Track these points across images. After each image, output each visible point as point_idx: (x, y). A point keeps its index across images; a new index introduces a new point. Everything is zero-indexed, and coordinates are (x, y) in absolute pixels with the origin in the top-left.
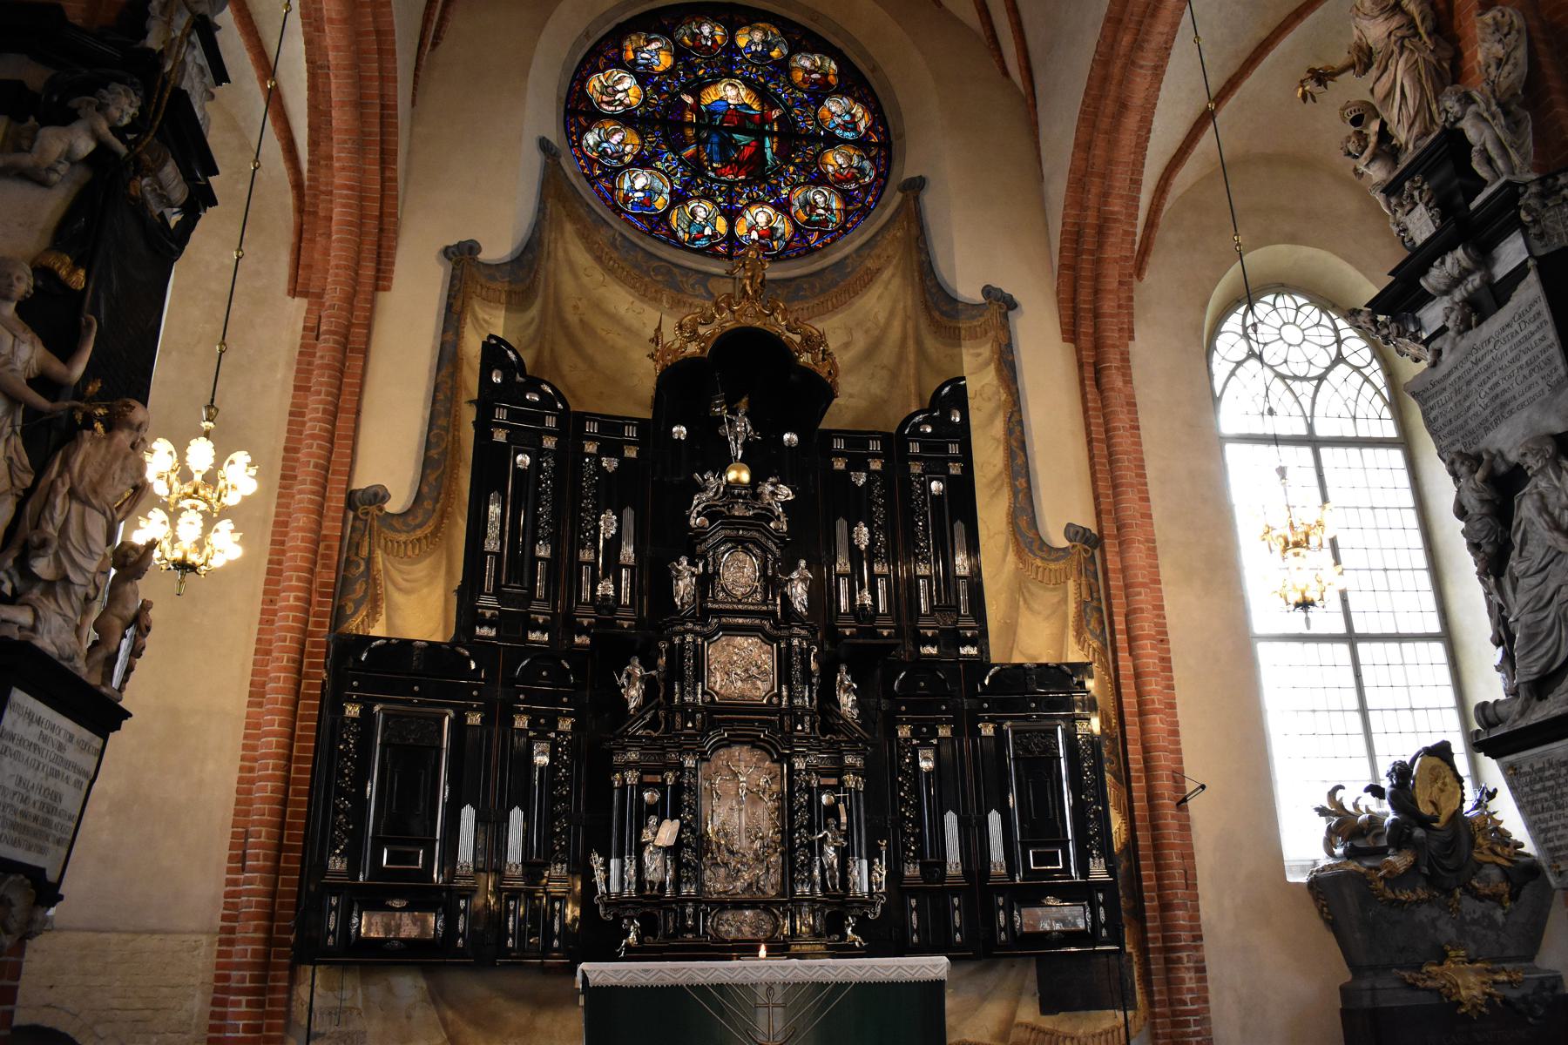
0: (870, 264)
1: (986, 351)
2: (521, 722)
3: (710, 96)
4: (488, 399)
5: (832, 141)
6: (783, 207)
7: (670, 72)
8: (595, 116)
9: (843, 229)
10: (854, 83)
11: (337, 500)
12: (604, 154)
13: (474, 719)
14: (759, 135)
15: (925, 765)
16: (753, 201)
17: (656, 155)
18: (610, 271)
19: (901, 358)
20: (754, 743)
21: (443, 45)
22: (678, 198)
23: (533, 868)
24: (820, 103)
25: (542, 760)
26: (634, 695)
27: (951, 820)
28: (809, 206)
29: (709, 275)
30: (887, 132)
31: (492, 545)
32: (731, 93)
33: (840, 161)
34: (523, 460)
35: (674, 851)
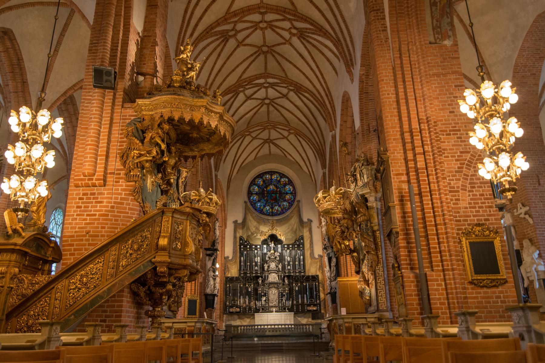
1: (307, 229)
2: (247, 286)
3: (268, 189)
4: (241, 245)
5: (287, 193)
6: (280, 206)
7: (262, 185)
8: (252, 194)
9: (289, 209)
11: (223, 259)
13: (242, 286)
14: (276, 194)
16: (275, 206)
21: (230, 188)
22: (265, 206)
23: (249, 303)
26: (260, 282)
27: (300, 296)
28: (284, 205)
29: (268, 220)
31: (242, 264)
32: (272, 187)
34: (245, 252)
35: (265, 300)
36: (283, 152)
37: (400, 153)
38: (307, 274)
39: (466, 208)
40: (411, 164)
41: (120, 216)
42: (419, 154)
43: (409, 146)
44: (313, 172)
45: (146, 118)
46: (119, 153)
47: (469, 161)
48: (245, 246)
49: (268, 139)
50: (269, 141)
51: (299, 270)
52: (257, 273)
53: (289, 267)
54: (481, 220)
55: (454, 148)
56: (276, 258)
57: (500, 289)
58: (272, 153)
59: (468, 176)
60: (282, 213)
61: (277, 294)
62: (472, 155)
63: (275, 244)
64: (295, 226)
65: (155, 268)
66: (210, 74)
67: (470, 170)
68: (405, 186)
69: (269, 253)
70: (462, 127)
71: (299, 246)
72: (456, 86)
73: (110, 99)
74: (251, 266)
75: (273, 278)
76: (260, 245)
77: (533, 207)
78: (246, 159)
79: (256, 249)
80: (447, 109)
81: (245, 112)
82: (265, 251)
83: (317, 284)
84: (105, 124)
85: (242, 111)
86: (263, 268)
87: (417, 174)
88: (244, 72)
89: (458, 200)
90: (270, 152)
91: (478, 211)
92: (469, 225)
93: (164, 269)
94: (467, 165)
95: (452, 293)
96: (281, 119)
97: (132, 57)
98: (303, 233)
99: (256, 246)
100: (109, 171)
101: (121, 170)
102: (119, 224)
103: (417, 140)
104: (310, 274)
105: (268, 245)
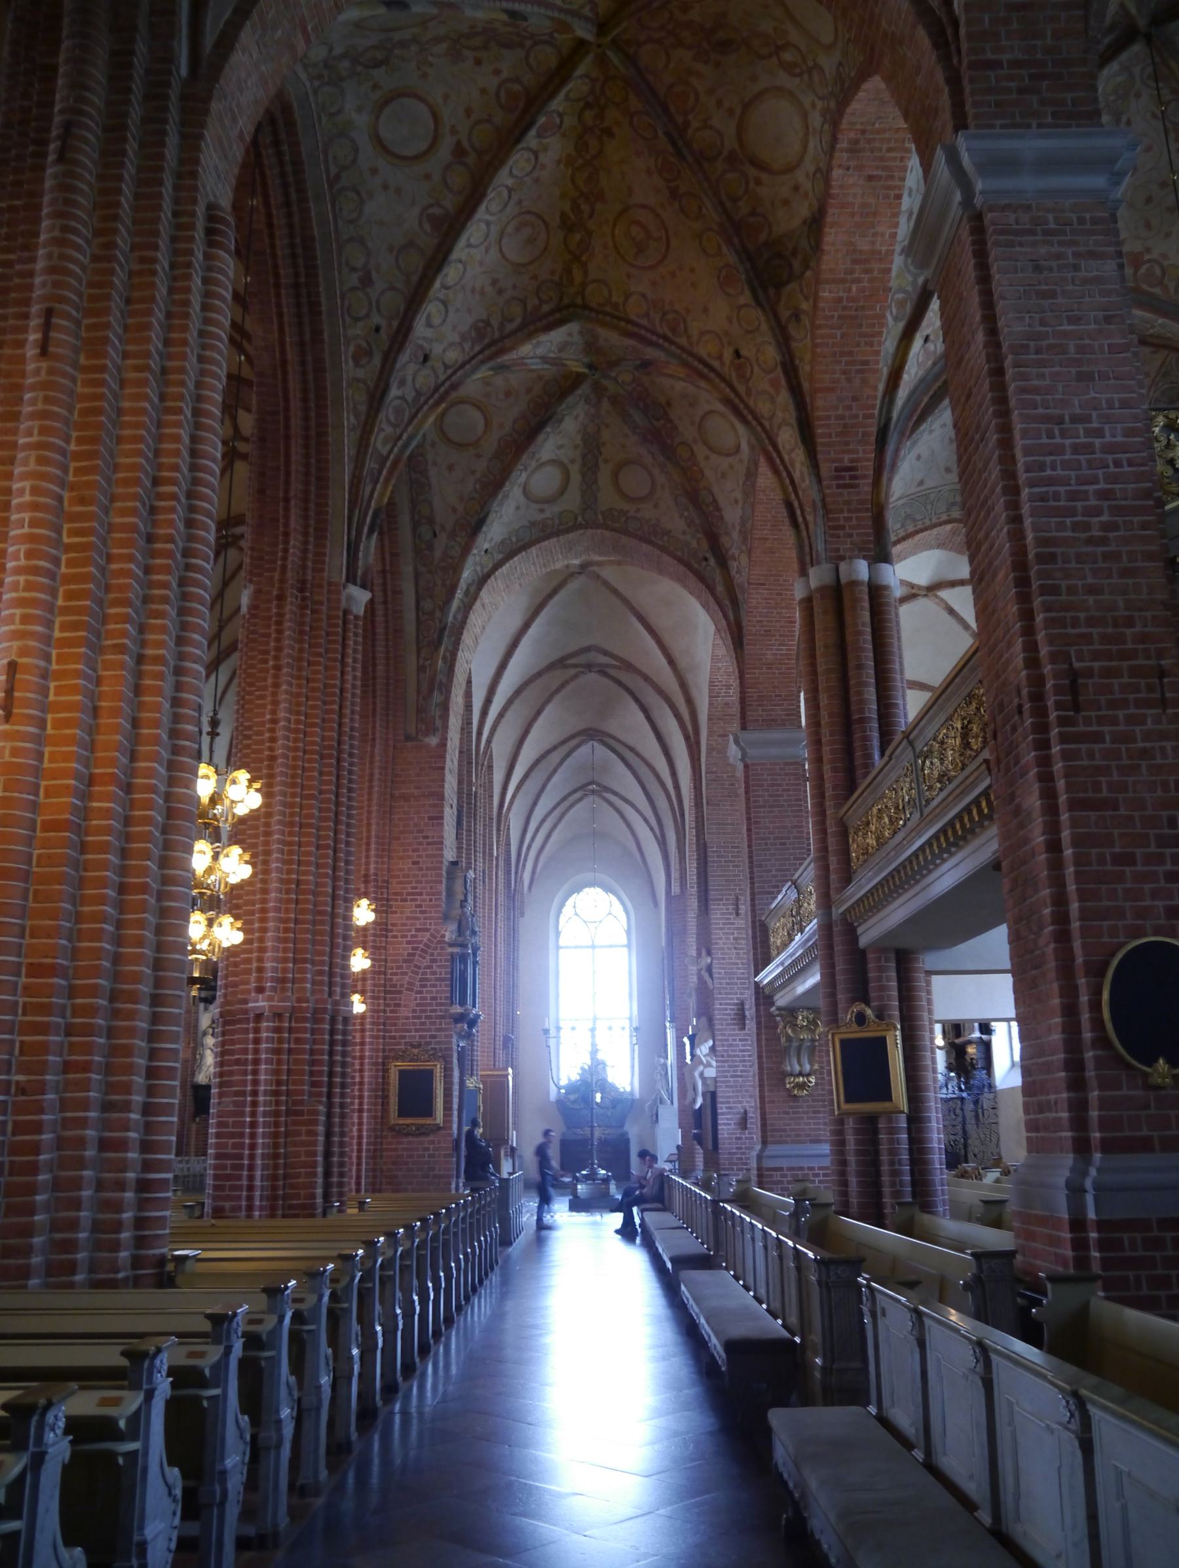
39: (407, 1018)
47: (426, 945)
54: (425, 1037)
55: (409, 922)
57: (431, 1138)
59: (419, 968)
62: (432, 935)
67: (424, 958)
70: (425, 888)
72: (430, 818)
77: (718, 959)
80: (409, 857)
89: (398, 1005)
91: (423, 1024)
92: (406, 1043)
94: (422, 950)
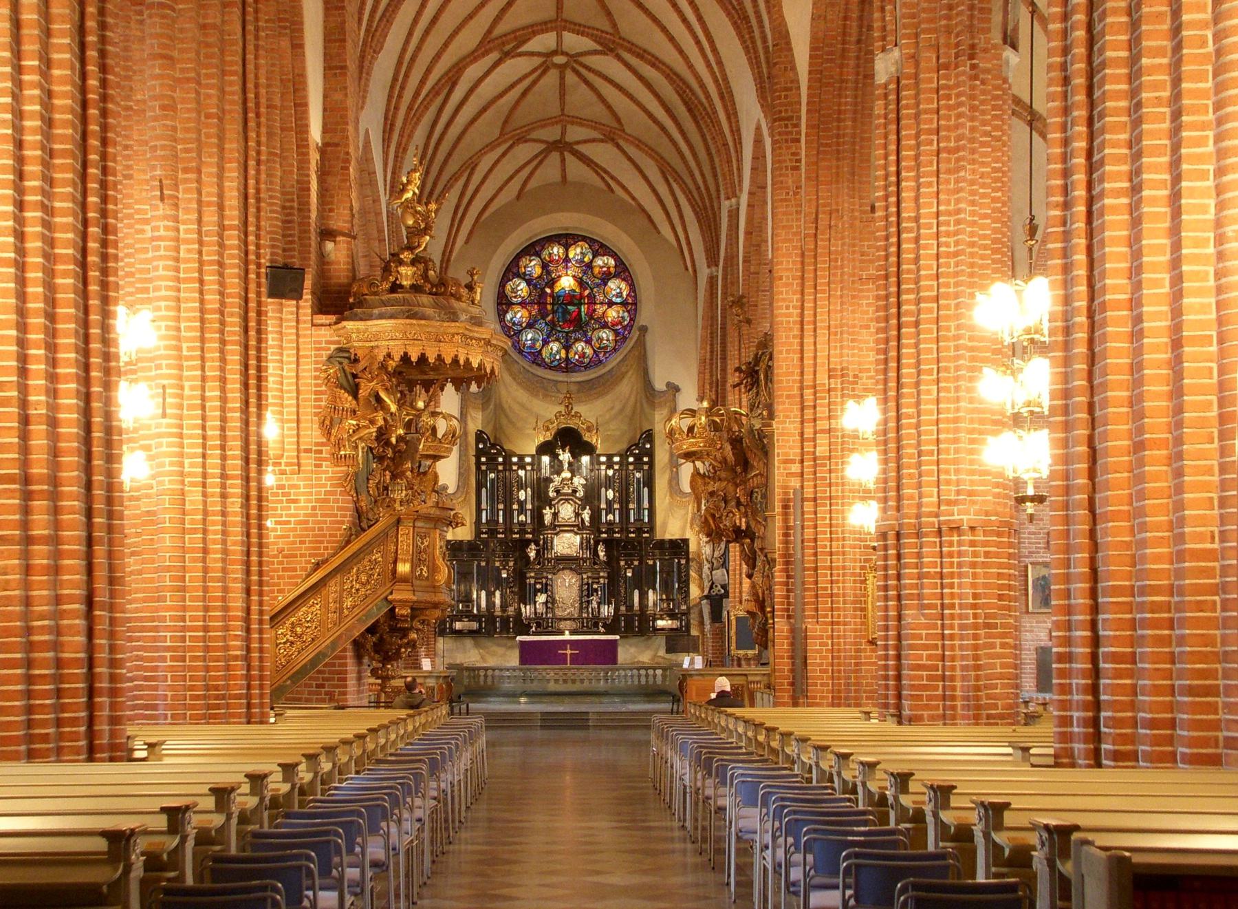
0: (624, 369)
4: (479, 454)
5: (611, 304)
6: (589, 342)
7: (540, 277)
8: (510, 304)
9: (615, 350)
10: (622, 271)
12: (514, 324)
15: (629, 574)
16: (577, 340)
17: (536, 321)
18: (519, 384)
19: (634, 412)
20: (571, 569)
24: (606, 284)
25: (504, 575)
26: (532, 555)
27: (636, 593)
28: (600, 339)
29: (557, 382)
30: (635, 297)
31: (484, 506)
33: (614, 314)
34: (492, 475)
36: (603, 178)
37: (794, 422)
38: (658, 536)
40: (808, 447)
41: (325, 522)
42: (823, 431)
43: (808, 414)
44: (689, 243)
45: (360, 354)
46: (316, 414)
48: (492, 460)
49: (559, 141)
50: (560, 146)
51: (638, 525)
52: (523, 531)
53: (610, 517)
56: (575, 491)
58: (570, 178)
60: (596, 362)
61: (576, 588)
63: (574, 456)
64: (633, 399)
65: (393, 609)
66: (410, 34)
68: (795, 483)
69: (557, 479)
71: (638, 459)
73: (292, 313)
74: (508, 513)
75: (567, 544)
76: (532, 456)
78: (491, 200)
79: (522, 465)
81: (495, 93)
82: (546, 471)
83: (683, 562)
84: (289, 363)
85: (487, 89)
86: (538, 516)
87: (815, 466)
88: (497, 19)
90: (564, 177)
93: (406, 611)
95: (952, 627)
96: (599, 112)
97: (314, 214)
98: (652, 423)
99: (521, 458)
100: (302, 447)
101: (323, 444)
102: (325, 536)
103: (822, 405)
104: (668, 537)
105: (554, 456)
